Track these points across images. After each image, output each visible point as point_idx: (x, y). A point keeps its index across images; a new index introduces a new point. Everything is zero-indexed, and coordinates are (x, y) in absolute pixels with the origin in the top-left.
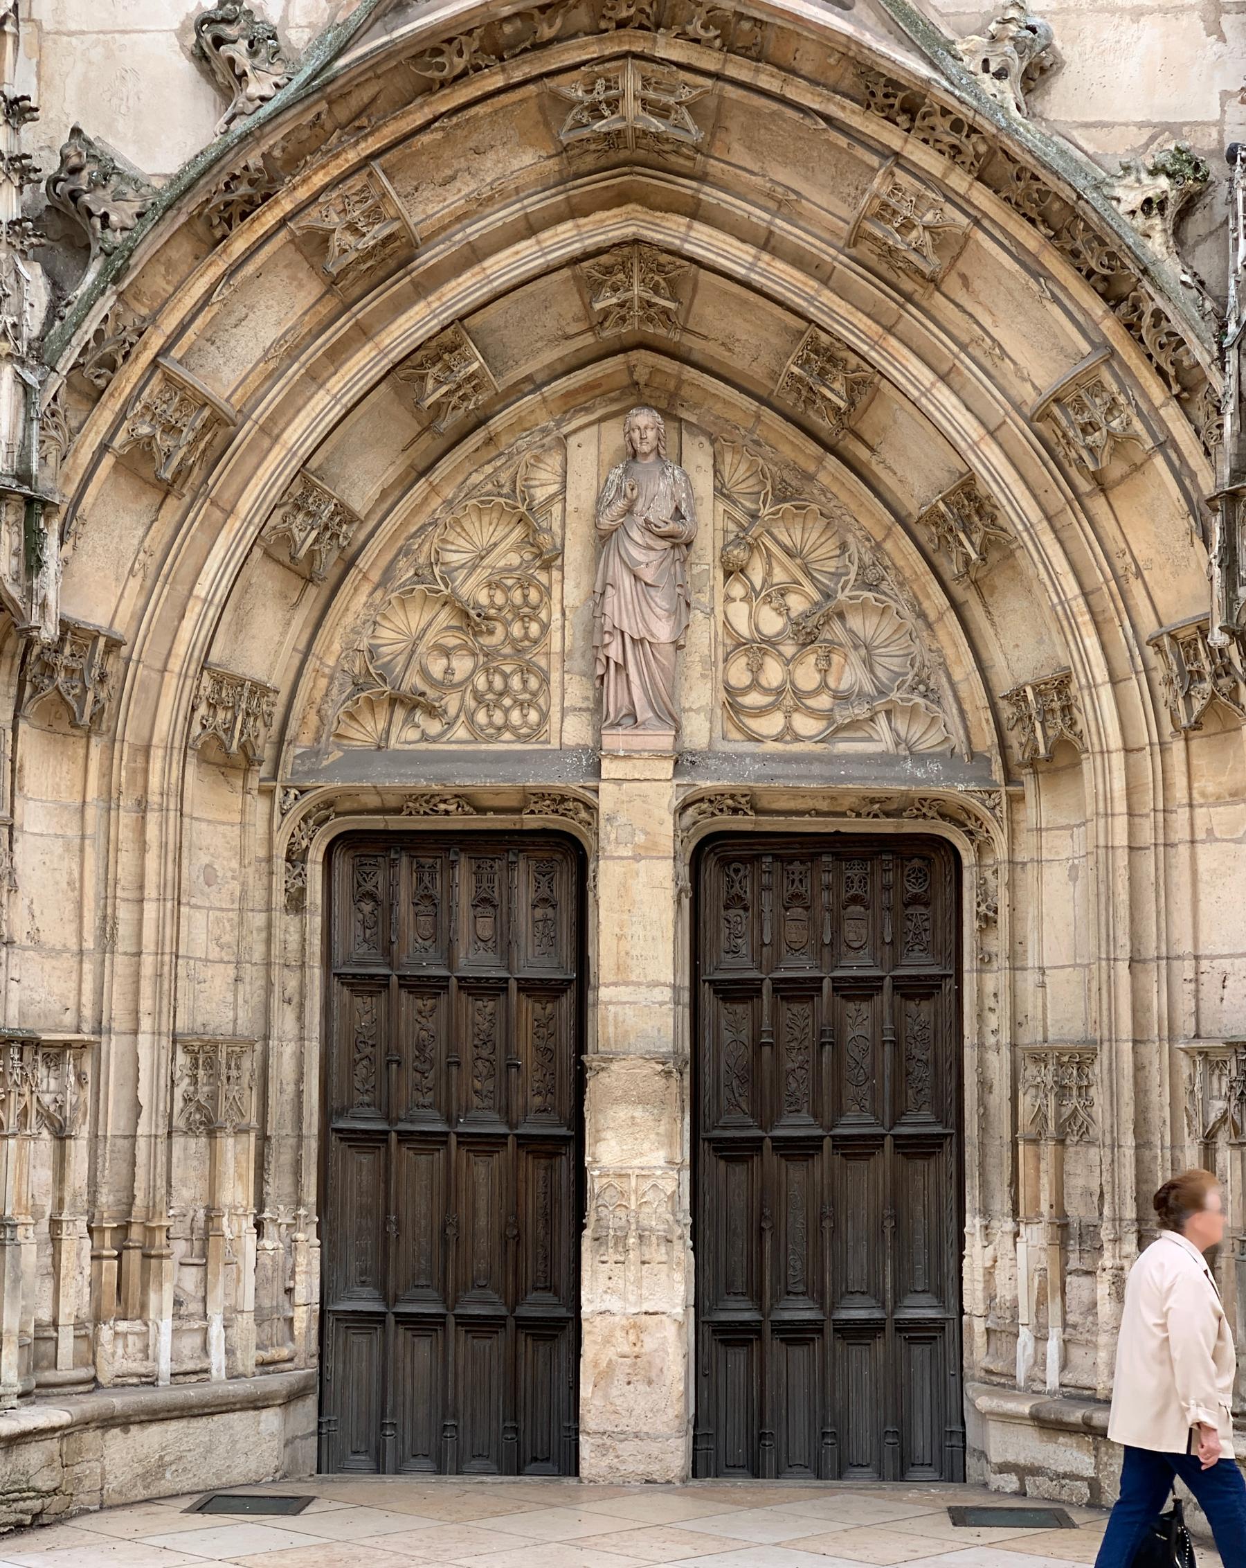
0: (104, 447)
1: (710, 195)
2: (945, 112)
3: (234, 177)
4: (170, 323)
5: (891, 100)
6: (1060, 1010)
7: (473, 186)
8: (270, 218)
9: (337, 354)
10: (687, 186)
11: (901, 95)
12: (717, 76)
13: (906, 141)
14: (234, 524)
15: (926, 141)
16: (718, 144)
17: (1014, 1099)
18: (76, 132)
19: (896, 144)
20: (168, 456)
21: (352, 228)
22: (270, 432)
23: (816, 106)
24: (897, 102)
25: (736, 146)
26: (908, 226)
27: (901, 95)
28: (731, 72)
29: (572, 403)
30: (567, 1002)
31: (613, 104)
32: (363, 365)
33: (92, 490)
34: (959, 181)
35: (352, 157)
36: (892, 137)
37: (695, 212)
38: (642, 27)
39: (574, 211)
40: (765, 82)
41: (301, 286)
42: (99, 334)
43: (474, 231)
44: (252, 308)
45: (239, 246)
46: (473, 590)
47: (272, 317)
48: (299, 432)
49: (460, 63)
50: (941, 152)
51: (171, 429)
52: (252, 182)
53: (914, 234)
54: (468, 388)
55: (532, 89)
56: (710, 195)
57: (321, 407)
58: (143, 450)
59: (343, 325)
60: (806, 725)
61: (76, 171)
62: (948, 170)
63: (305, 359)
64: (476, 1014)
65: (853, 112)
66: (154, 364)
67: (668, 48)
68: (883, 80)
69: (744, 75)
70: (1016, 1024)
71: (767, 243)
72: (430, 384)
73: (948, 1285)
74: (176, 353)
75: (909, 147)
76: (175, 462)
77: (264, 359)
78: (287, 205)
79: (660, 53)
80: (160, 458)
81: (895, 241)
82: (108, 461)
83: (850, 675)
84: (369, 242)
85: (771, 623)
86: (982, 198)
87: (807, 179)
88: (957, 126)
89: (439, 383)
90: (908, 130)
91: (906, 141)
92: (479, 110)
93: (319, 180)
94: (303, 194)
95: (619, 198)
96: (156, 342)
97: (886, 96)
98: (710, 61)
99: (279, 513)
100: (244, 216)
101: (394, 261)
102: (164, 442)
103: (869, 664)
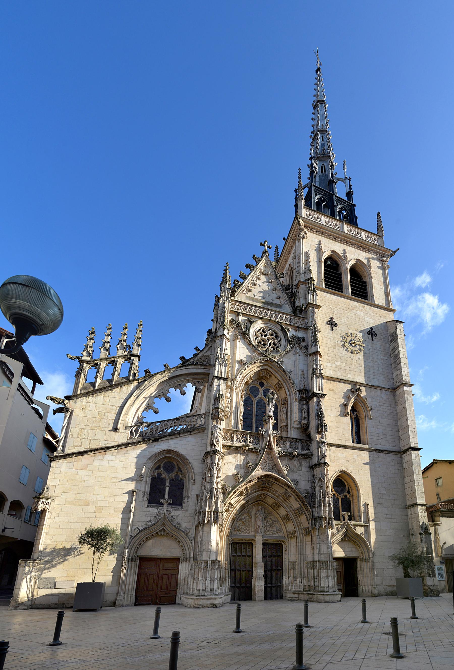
1: (270, 491)
6: (293, 558)
10: (268, 490)
17: (288, 566)
29: (253, 505)
30: (251, 558)
37: (268, 491)
46: (244, 520)
56: (270, 491)
60: (270, 533)
64: (243, 559)
70: (289, 559)
71: (274, 494)
73: (281, 582)
83: (274, 529)
85: (268, 524)
95: (263, 490)
98: (273, 481)
103: (276, 528)
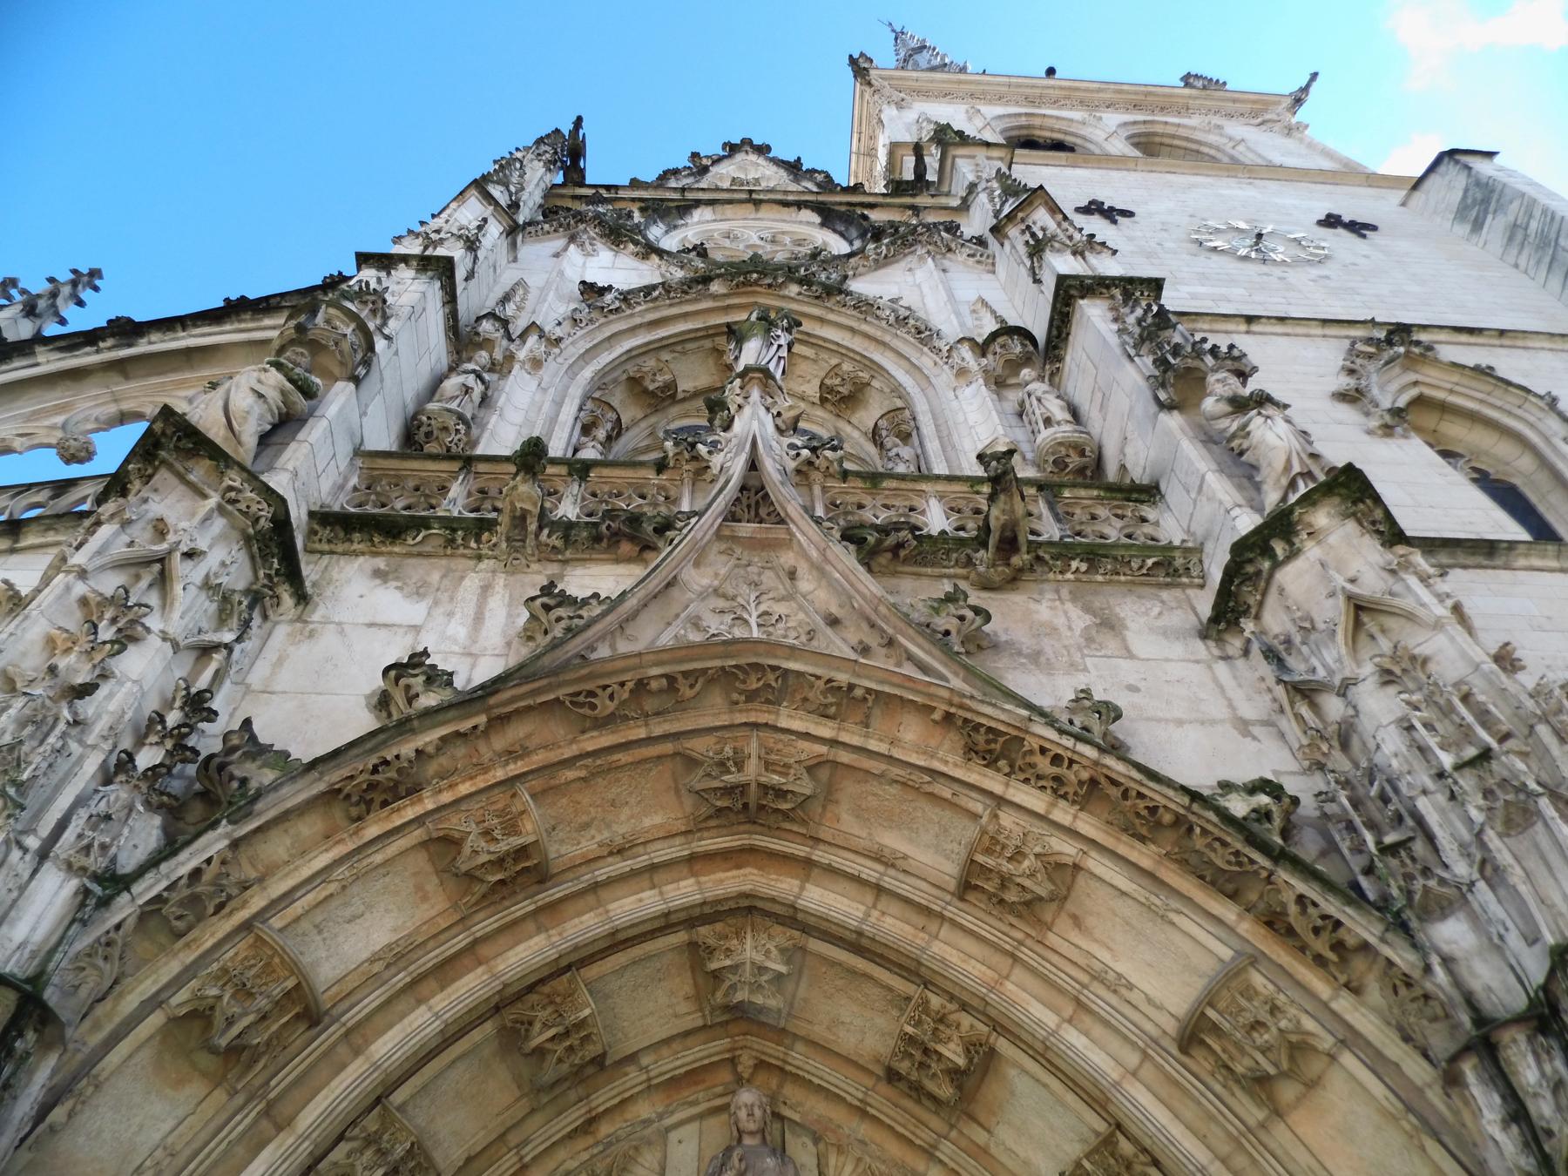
0: (154, 1002)
2: (1043, 751)
3: (386, 763)
4: (278, 888)
5: (993, 746)
7: (606, 834)
8: (410, 813)
9: (445, 971)
11: (1001, 740)
12: (833, 743)
13: (1007, 785)
14: (286, 1140)
15: (1026, 781)
16: (829, 815)
18: (247, 723)
20: (230, 1022)
21: (487, 833)
22: (357, 1038)
23: (922, 763)
24: (998, 747)
25: (845, 816)
26: (1018, 855)
27: (1001, 740)
28: (845, 737)
31: (740, 766)
32: (471, 987)
33: (124, 1048)
34: (1063, 814)
35: (500, 774)
36: (993, 782)
38: (768, 701)
39: (695, 862)
40: (873, 745)
41: (425, 898)
42: (196, 874)
43: (603, 872)
44: (369, 907)
45: (372, 831)
47: (389, 922)
48: (389, 1046)
49: (611, 706)
50: (1043, 788)
51: (244, 992)
52: (399, 771)
53: (1026, 863)
54: (573, 1040)
55: (668, 748)
57: (419, 1023)
58: (201, 1015)
59: (461, 941)
61: (234, 749)
62: (1053, 805)
63: (412, 971)
65: (956, 765)
66: (247, 926)
67: (790, 719)
68: (982, 730)
69: (856, 740)
72: (537, 1026)
74: (277, 922)
75: (1011, 791)
76: (235, 1031)
77: (372, 960)
78: (429, 805)
80: (219, 1021)
81: (1007, 867)
82: (156, 1020)
84: (503, 847)
86: (1087, 825)
87: (911, 840)
88: (1056, 760)
89: (546, 1026)
91: (1007, 785)
92: (623, 757)
93: (465, 788)
94: (447, 797)
96: (257, 902)
97: (988, 742)
99: (344, 1147)
100: (385, 804)
101: (524, 872)
102: (228, 1004)
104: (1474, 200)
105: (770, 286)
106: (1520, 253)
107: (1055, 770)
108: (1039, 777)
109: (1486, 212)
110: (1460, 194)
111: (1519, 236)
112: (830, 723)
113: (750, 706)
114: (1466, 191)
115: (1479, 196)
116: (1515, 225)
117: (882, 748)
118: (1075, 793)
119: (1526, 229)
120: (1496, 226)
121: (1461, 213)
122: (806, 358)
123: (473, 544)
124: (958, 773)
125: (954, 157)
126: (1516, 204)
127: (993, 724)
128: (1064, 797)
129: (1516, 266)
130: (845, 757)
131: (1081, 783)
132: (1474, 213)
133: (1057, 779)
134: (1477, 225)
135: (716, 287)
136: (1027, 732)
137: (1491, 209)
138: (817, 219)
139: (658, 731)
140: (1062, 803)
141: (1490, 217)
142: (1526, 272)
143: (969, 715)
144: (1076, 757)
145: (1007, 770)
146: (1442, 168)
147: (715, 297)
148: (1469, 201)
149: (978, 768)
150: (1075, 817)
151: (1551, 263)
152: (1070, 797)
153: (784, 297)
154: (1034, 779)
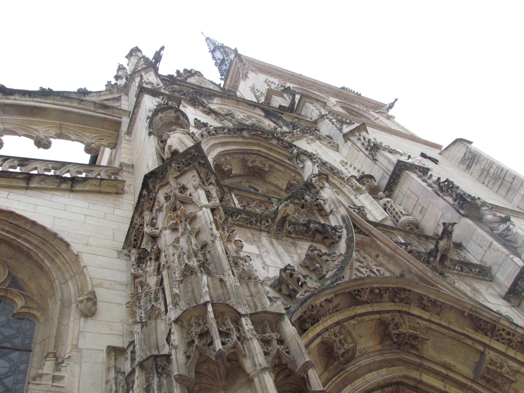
2: (503, 330)
11: (489, 325)
13: (490, 341)
15: (498, 340)
19: (487, 342)
28: (433, 319)
34: (511, 353)
50: (504, 343)
62: (507, 349)
65: (472, 333)
69: (437, 321)
79: (412, 311)
88: (508, 333)
90: (491, 338)
91: (490, 341)
104: (468, 158)
105: (266, 138)
106: (485, 179)
107: (508, 337)
108: (503, 339)
109: (473, 163)
110: (463, 154)
111: (485, 173)
112: (428, 314)
113: (400, 304)
114: (465, 154)
115: (470, 156)
116: (484, 169)
117: (446, 324)
118: (517, 346)
119: (488, 171)
120: (476, 169)
121: (463, 161)
122: (280, 170)
123: (258, 224)
124: (473, 336)
125: (305, 102)
126: (485, 162)
127: (485, 319)
128: (512, 347)
129: (483, 183)
130: (433, 327)
131: (518, 342)
132: (468, 162)
133: (509, 340)
134: (469, 167)
135: (245, 133)
136: (498, 322)
137: (475, 162)
138: (263, 114)
139: (376, 309)
140: (510, 349)
141: (474, 165)
142: (487, 186)
143: (477, 315)
144: (515, 333)
145: (490, 336)
146: (457, 144)
147: (244, 137)
148: (466, 158)
149: (480, 335)
150: (515, 354)
151: (500, 185)
152: (514, 347)
153: (271, 144)
154: (500, 339)
